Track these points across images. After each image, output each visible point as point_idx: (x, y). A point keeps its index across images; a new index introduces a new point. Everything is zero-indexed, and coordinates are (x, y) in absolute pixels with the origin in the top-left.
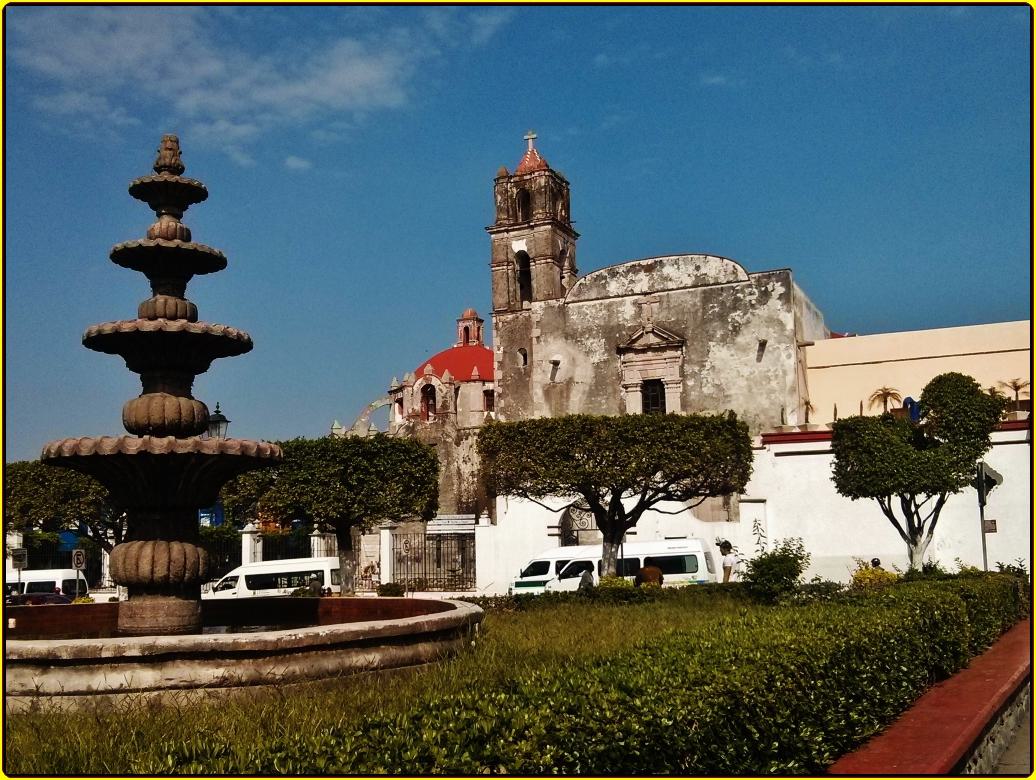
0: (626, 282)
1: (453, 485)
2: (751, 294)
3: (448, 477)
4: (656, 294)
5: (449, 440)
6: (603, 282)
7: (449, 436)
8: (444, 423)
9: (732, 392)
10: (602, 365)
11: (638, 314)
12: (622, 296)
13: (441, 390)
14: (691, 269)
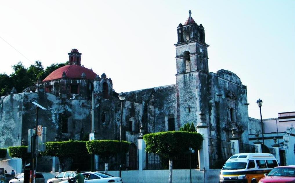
1: (114, 130)
3: (112, 126)
5: (113, 110)
7: (113, 108)
8: (111, 102)
9: (242, 116)
12: (227, 80)
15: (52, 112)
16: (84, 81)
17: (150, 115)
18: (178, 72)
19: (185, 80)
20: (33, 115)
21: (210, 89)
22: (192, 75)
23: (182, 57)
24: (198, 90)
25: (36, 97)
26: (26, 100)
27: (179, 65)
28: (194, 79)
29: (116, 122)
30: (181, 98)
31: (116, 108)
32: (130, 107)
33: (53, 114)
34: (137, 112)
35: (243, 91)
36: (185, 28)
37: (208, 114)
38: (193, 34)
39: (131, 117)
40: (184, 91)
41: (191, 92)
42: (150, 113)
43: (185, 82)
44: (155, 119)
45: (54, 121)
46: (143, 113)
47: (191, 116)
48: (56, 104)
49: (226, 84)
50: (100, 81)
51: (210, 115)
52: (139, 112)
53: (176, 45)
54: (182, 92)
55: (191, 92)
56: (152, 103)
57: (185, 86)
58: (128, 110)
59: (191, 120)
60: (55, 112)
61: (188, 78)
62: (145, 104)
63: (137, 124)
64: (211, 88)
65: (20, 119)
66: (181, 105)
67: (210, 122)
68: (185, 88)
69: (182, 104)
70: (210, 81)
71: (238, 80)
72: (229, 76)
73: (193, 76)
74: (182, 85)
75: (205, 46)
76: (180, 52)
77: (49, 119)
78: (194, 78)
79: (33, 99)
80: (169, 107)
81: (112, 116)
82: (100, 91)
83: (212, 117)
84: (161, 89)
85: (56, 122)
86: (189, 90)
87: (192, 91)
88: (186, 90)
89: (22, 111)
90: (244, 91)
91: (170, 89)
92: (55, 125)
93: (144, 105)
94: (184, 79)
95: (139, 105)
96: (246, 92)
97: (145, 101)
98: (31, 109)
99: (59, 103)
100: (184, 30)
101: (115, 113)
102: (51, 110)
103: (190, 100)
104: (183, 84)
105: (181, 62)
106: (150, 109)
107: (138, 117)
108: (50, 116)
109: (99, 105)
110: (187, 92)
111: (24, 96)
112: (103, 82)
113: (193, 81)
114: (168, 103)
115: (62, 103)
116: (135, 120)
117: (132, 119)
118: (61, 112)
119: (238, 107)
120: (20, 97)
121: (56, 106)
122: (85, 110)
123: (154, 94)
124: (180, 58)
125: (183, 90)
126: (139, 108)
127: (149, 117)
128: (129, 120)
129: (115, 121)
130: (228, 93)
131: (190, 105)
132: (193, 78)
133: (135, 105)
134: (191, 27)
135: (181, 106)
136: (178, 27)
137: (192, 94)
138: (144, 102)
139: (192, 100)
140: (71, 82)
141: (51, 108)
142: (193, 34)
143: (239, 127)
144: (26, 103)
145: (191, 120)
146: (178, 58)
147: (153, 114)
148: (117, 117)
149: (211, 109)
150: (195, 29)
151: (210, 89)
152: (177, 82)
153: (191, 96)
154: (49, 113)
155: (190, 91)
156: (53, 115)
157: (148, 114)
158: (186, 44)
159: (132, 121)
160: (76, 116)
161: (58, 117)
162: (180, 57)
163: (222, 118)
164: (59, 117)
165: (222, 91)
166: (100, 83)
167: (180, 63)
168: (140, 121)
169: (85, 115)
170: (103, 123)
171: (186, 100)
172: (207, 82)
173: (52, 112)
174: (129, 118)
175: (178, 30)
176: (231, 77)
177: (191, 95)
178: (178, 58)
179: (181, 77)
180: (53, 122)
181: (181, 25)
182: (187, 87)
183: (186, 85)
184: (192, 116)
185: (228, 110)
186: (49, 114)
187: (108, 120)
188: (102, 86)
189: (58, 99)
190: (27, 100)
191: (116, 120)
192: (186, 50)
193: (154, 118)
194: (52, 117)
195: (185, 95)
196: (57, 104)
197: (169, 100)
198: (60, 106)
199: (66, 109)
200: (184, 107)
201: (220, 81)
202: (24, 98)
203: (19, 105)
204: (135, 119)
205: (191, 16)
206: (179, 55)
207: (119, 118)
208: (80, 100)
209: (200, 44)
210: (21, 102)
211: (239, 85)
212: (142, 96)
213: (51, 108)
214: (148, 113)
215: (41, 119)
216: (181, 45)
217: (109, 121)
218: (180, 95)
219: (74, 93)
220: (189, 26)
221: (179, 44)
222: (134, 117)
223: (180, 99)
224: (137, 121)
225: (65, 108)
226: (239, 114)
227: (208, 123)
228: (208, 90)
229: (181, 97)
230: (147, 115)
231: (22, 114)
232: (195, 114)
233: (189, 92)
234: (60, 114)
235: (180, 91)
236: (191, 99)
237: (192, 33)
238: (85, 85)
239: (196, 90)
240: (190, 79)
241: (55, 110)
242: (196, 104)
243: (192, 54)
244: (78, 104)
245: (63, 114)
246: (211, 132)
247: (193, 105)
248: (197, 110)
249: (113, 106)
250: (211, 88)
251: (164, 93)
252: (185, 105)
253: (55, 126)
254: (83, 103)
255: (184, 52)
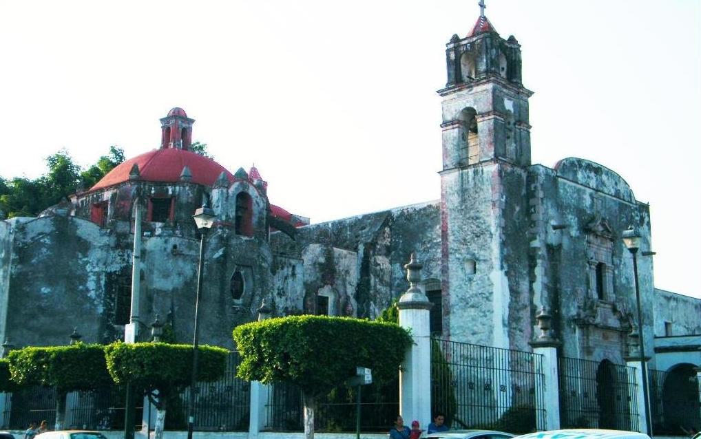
0: (586, 176)
2: (637, 216)
4: (601, 194)
6: (575, 169)
8: (260, 243)
10: (577, 240)
11: (592, 205)
12: (586, 187)
13: (257, 203)
14: (614, 182)
15: (88, 270)
16: (187, 188)
17: (377, 280)
18: (447, 166)
19: (464, 186)
20: (37, 277)
21: (533, 210)
22: (482, 171)
23: (457, 125)
24: (498, 211)
25: (48, 230)
26: (21, 236)
27: (449, 147)
28: (487, 183)
29: (273, 300)
30: (454, 235)
31: (274, 261)
32: (322, 260)
33: (90, 274)
34: (343, 273)
35: (637, 218)
36: (466, 45)
37: (527, 279)
38: (487, 59)
39: (323, 287)
40: (461, 216)
41: (477, 218)
42: (377, 276)
43: (463, 191)
44: (393, 292)
45: (92, 294)
46: (359, 277)
47: (477, 284)
48: (100, 247)
49: (585, 197)
50: (228, 188)
51: (532, 281)
52: (347, 272)
53: (442, 93)
54: (455, 219)
55: (477, 218)
56: (384, 251)
57: (463, 201)
58: (316, 268)
59: (476, 295)
60: (97, 269)
61: (470, 179)
62: (364, 253)
63: (341, 305)
64: (534, 206)
65: (4, 288)
66: (451, 253)
67: (531, 302)
68: (464, 207)
69: (456, 250)
70: (533, 189)
71: (621, 187)
72: (592, 174)
73: (485, 175)
74: (455, 200)
75: (522, 95)
76: (453, 109)
77: (81, 287)
78: (487, 180)
79: (39, 234)
80: (426, 261)
81: (263, 282)
82: (227, 216)
83: (538, 286)
84: (408, 212)
85: (98, 296)
86: (472, 213)
87: (481, 215)
88: (465, 214)
89: (10, 265)
90: (642, 219)
91: (431, 213)
92: (96, 303)
93: (363, 256)
94: (460, 184)
95: (349, 256)
96: (646, 220)
97: (365, 244)
98: (33, 261)
99: (109, 245)
100: (464, 52)
101: (270, 274)
102: (87, 262)
103: (476, 239)
104: (459, 195)
105: (455, 138)
106: (379, 265)
107: (345, 287)
108: (83, 279)
109: (224, 252)
110: (469, 219)
111: (17, 228)
112: (237, 193)
113: (484, 187)
114: (424, 251)
115: (117, 246)
116: (335, 296)
117: (325, 292)
118: (113, 270)
119: (621, 261)
120: (7, 228)
121: (100, 252)
122: (181, 263)
123: (390, 227)
124: (451, 127)
125: (457, 214)
126: (349, 262)
127: (375, 286)
128: (317, 293)
129: (270, 295)
130: (590, 222)
131: (476, 252)
132: (485, 180)
133: (336, 255)
134: (482, 42)
135: (451, 257)
136: (447, 45)
137: (480, 223)
138: (361, 248)
139: (481, 241)
140: (153, 192)
141: (85, 259)
142: (485, 60)
143: (621, 317)
144: (21, 245)
145: (476, 295)
146: (448, 128)
147: (387, 278)
148: (277, 286)
149: (535, 265)
150: (492, 48)
151: (533, 210)
152: (444, 192)
153: (478, 229)
154: (79, 272)
155: (477, 214)
156: (89, 277)
157: (372, 281)
158: (467, 88)
159: (327, 298)
160: (155, 279)
161: (103, 282)
162: (453, 124)
163: (569, 289)
164: (106, 282)
165: (570, 217)
166: (228, 193)
167: (450, 141)
168: (352, 297)
169: (181, 278)
170: (236, 301)
171: (465, 240)
172: (524, 192)
173: (88, 268)
174: (318, 288)
175: (448, 51)
176: (601, 180)
177: (478, 226)
178: (446, 126)
179: (454, 176)
180: (89, 295)
181: (456, 39)
182: (468, 204)
183: (465, 200)
184: (479, 282)
185: (587, 269)
186: (80, 276)
187: (251, 293)
188: (233, 201)
189: (105, 234)
190: (24, 238)
191: (275, 294)
192: (468, 105)
193: (391, 290)
194: (86, 281)
195: (464, 226)
196: (101, 248)
197: (429, 242)
198: (111, 252)
199: (128, 262)
200: (459, 259)
201: (565, 189)
202: (16, 232)
203: (4, 251)
204: (335, 290)
205: (486, 14)
206: (449, 118)
207: (283, 289)
208: (167, 238)
209: (506, 88)
210: (8, 241)
211: (624, 200)
212: (360, 232)
213: (86, 259)
214: (372, 276)
215: (59, 288)
216: (454, 92)
217: (253, 295)
218: (449, 226)
219: (159, 221)
220: (477, 40)
221: (449, 89)
222: (332, 285)
223: (451, 238)
224: (340, 297)
225: (124, 260)
226: (624, 281)
227: (528, 303)
228: (528, 211)
229: (453, 231)
230: (369, 281)
231: (9, 273)
232: (489, 279)
233: (473, 218)
234: (109, 275)
235: (451, 216)
236: (477, 236)
237: (482, 59)
238: (190, 201)
239: (492, 212)
240: (475, 183)
241: (97, 264)
242: (492, 251)
243: (483, 115)
244: (163, 248)
245: (118, 275)
246: (535, 327)
247: (482, 252)
248: (493, 268)
249: (266, 254)
250: (537, 207)
251: (416, 224)
252: (461, 254)
253: (96, 306)
254: (175, 247)
255: (461, 109)
